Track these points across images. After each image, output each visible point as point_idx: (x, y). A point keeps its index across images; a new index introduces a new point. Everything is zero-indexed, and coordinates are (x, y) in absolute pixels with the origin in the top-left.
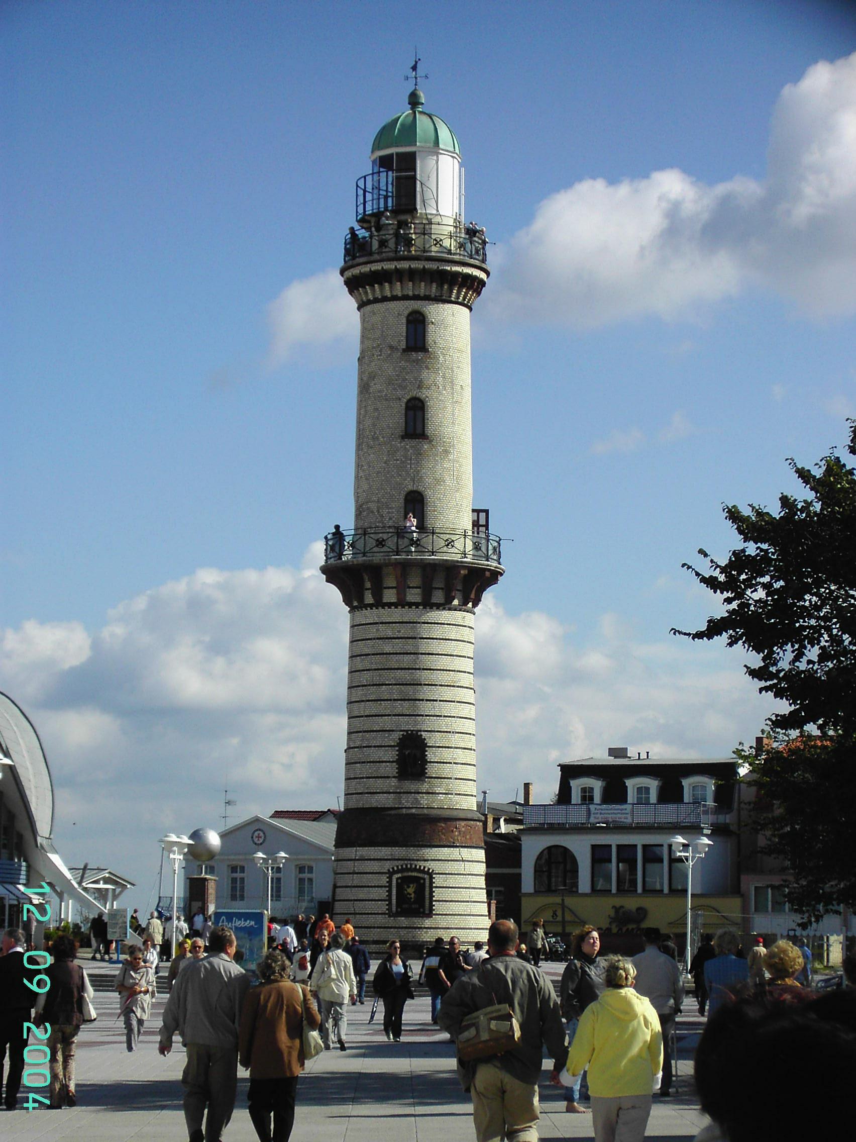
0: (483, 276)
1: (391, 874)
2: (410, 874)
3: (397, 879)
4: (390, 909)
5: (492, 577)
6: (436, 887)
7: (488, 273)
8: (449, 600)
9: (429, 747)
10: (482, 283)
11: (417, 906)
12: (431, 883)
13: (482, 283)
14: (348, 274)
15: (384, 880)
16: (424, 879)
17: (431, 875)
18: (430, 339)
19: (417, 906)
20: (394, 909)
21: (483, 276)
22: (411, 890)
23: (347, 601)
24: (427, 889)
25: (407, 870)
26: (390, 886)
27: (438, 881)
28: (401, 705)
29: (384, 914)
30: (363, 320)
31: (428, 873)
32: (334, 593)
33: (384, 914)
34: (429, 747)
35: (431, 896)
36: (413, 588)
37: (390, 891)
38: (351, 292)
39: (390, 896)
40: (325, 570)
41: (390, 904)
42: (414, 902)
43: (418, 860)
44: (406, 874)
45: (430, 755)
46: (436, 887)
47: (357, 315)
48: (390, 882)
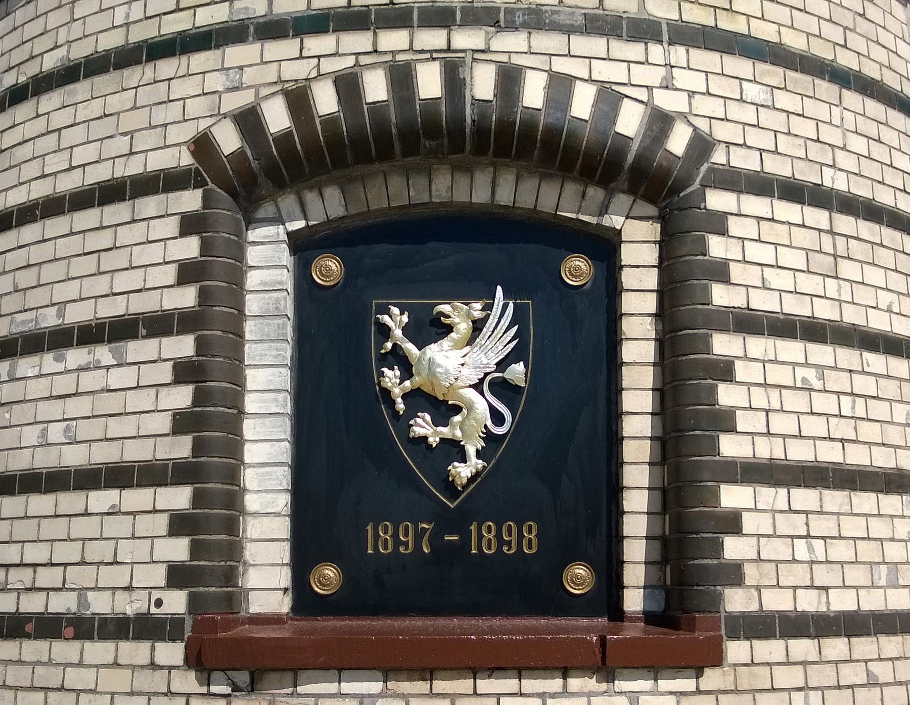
1: (242, 179)
2: (446, 188)
3: (303, 247)
4: (210, 561)
6: (747, 323)
12: (682, 276)
15: (144, 257)
20: (266, 580)
22: (465, 360)
24: (639, 349)
27: (762, 255)
29: (148, 628)
33: (148, 628)
37: (212, 383)
39: (212, 420)
41: (212, 525)
44: (393, 191)
46: (747, 323)
48: (215, 276)
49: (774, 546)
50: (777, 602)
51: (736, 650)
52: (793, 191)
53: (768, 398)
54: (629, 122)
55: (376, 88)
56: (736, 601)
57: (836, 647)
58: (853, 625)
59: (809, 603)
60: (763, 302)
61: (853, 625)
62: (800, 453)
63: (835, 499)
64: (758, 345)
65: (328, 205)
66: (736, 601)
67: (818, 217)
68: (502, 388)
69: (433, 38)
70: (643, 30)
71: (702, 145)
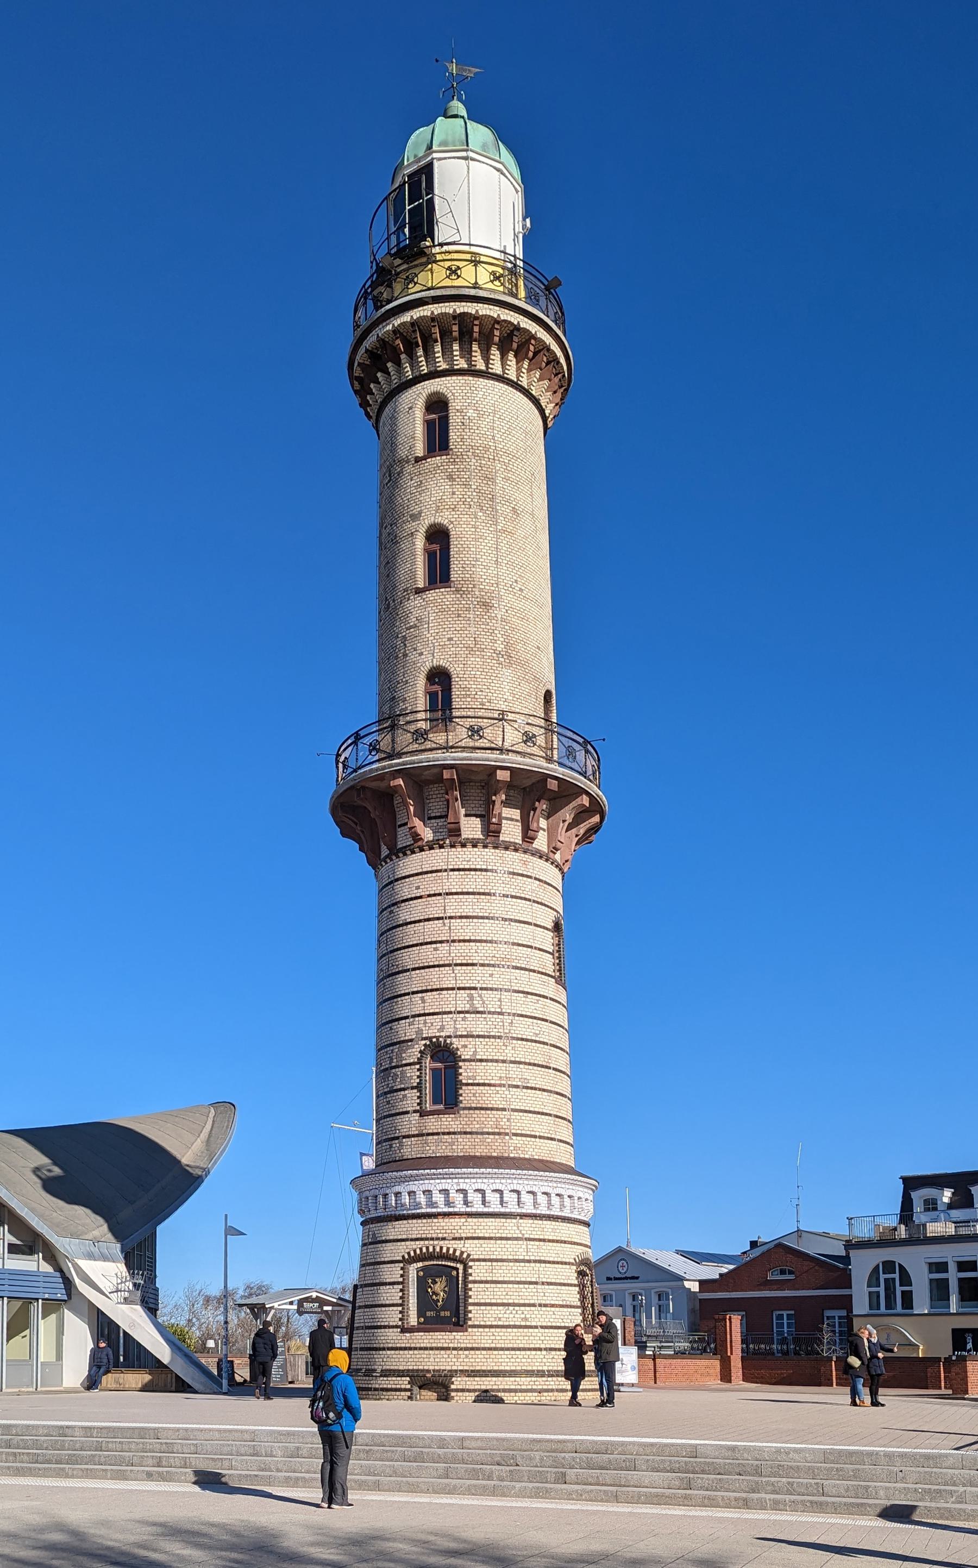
6: (475, 1282)
9: (464, 1060)
11: (448, 1314)
16: (457, 1269)
18: (453, 435)
19: (448, 1314)
25: (431, 1256)
26: (403, 1283)
27: (477, 1271)
28: (423, 1001)
31: (461, 1261)
34: (464, 1060)
35: (467, 1297)
36: (435, 818)
42: (444, 1308)
43: (444, 1239)
45: (466, 1072)
46: (475, 1282)
49: (476, 1315)
50: (477, 1323)
51: (470, 1330)
52: (484, 1260)
53: (477, 1293)
54: (458, 1253)
55: (424, 1250)
56: (470, 1323)
57: (487, 1330)
58: (491, 1327)
59: (482, 1323)
60: (478, 1279)
61: (491, 1327)
62: (482, 1301)
63: (488, 1308)
64: (476, 1285)
65: (420, 1264)
66: (470, 1323)
67: (489, 1263)
68: (444, 1291)
69: (431, 1242)
70: (461, 1239)
71: (469, 1255)
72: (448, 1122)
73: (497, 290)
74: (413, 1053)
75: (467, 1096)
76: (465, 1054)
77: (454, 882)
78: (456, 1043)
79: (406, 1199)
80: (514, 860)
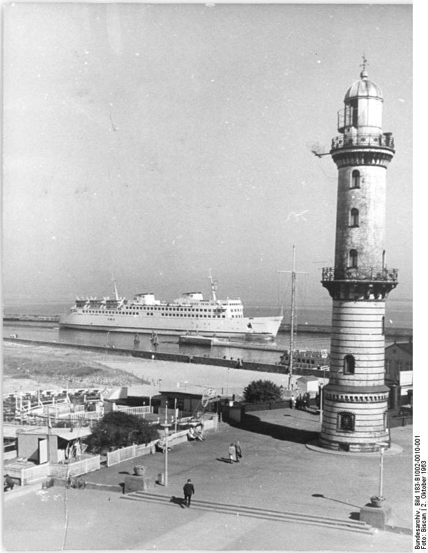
0: (391, 153)
5: (395, 285)
7: (394, 152)
8: (376, 297)
10: (391, 157)
13: (391, 157)
14: (335, 153)
17: (354, 415)
21: (391, 153)
23: (332, 294)
27: (357, 418)
30: (340, 173)
32: (326, 290)
38: (335, 161)
40: (323, 282)
45: (357, 364)
47: (337, 171)
49: (356, 428)
53: (357, 423)
72: (351, 377)
73: (376, 144)
74: (343, 357)
75: (357, 370)
76: (356, 359)
77: (359, 311)
78: (354, 356)
79: (340, 398)
80: (372, 304)
